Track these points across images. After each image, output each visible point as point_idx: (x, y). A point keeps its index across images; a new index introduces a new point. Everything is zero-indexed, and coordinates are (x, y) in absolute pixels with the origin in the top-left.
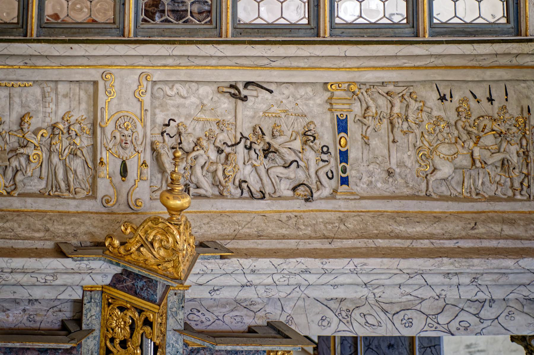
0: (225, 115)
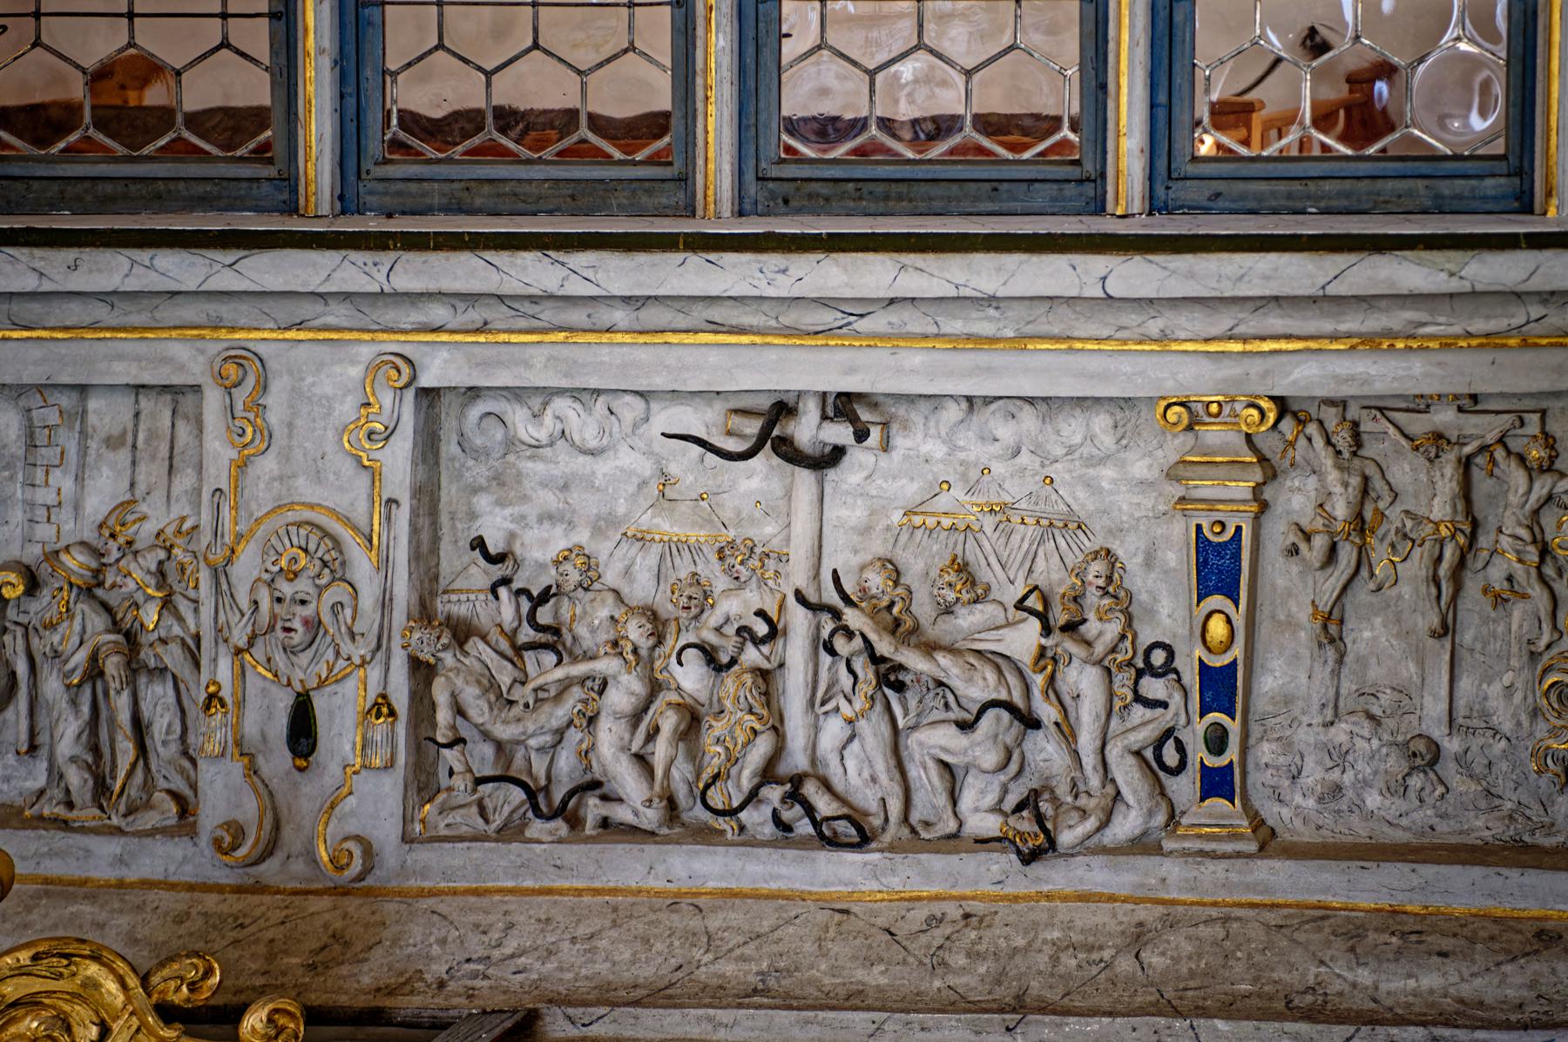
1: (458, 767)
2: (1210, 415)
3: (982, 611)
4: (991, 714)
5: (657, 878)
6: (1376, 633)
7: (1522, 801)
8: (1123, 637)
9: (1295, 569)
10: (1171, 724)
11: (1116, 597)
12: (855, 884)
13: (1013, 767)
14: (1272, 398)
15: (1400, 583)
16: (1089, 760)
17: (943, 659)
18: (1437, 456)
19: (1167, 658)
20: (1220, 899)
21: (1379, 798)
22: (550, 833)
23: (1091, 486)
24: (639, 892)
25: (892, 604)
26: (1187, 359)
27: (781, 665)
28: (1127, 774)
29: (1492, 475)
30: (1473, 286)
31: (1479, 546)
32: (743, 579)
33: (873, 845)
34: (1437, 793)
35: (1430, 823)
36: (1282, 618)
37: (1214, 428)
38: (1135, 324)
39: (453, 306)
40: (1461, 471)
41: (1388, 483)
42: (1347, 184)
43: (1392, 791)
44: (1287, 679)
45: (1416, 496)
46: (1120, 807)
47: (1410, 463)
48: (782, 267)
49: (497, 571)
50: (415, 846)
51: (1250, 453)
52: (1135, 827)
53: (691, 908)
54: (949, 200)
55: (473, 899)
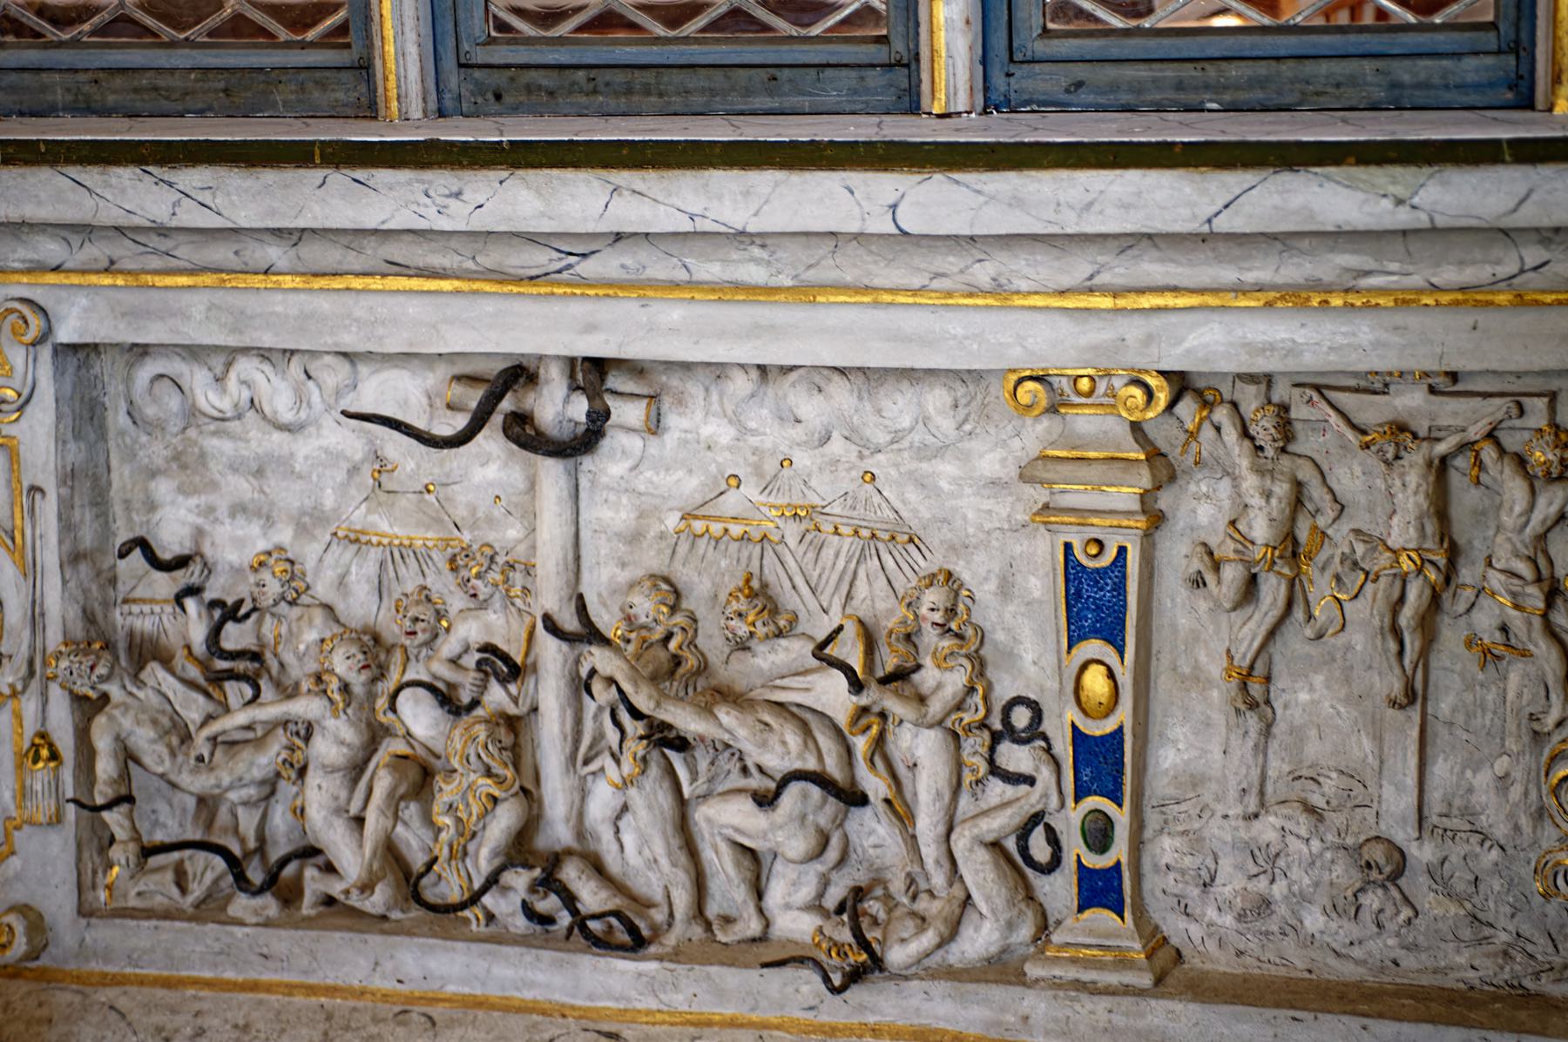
0: (490, 520)
1: (121, 834)
3: (787, 649)
4: (795, 788)
5: (384, 977)
6: (1316, 696)
8: (971, 690)
9: (1203, 606)
10: (1039, 807)
12: (629, 1000)
13: (832, 854)
15: (1348, 628)
16: (930, 851)
17: (726, 715)
18: (1397, 457)
19: (1032, 719)
21: (1322, 919)
22: (256, 913)
23: (922, 483)
24: (362, 993)
25: (668, 637)
26: (1039, 317)
27: (535, 710)
28: (979, 873)
29: (1478, 482)
30: (1432, 220)
31: (1461, 581)
32: (481, 597)
33: (652, 949)
35: (1393, 955)
36: (1187, 670)
38: (956, 270)
39: (65, 239)
40: (1432, 479)
41: (1331, 491)
42: (1262, 69)
43: (1340, 909)
44: (1194, 753)
46: (971, 916)
47: (1361, 464)
48: (455, 189)
49: (182, 578)
50: (93, 921)
52: (990, 944)
53: (423, 1019)
54: (713, 92)
55: (160, 993)
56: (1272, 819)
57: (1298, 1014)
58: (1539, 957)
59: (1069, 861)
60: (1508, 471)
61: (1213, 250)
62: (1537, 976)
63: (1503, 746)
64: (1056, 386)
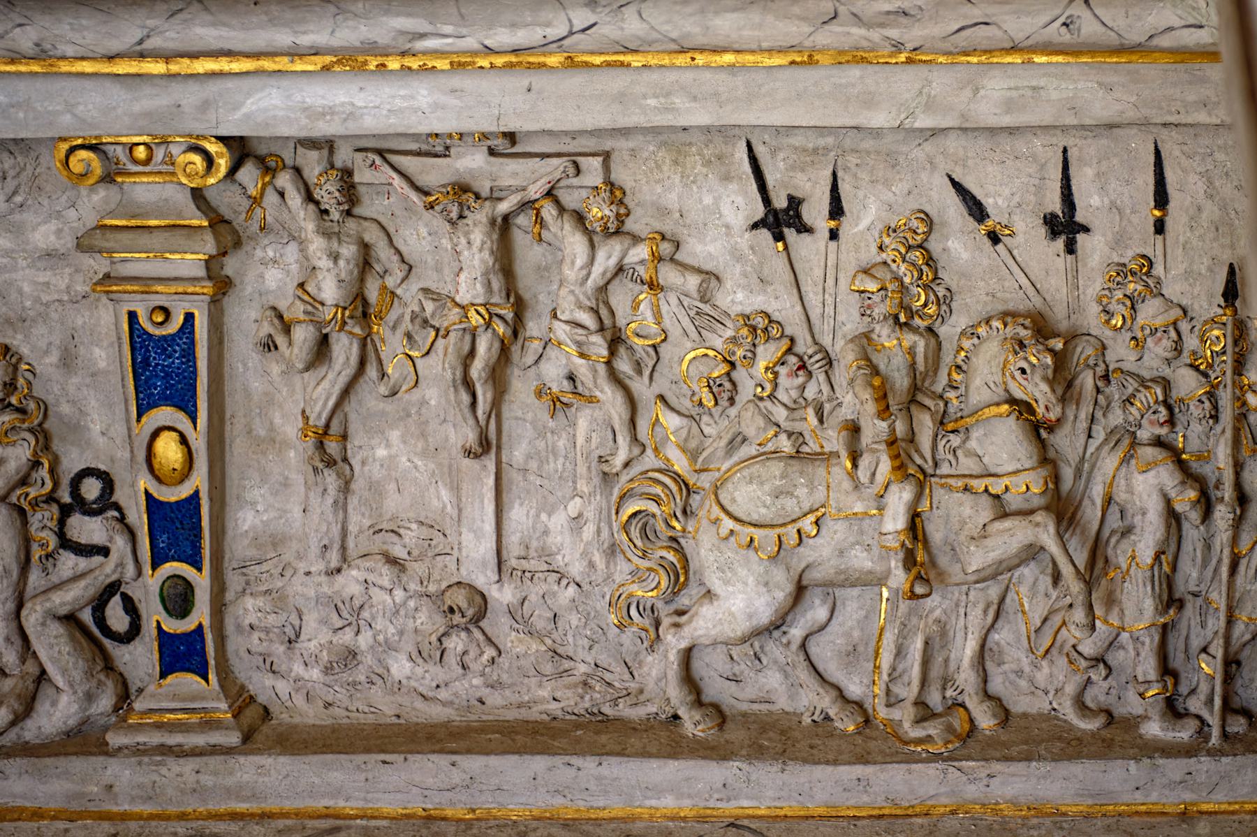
2: (135, 161)
6: (393, 451)
7: (599, 662)
8: (36, 464)
9: (276, 369)
10: (114, 578)
11: (22, 411)
14: (221, 139)
15: (422, 383)
18: (461, 217)
19: (103, 490)
20: (190, 810)
21: (408, 665)
26: (88, 84)
29: (541, 240)
31: (528, 334)
34: (486, 657)
35: (478, 695)
36: (262, 433)
37: (145, 179)
40: (495, 236)
43: (425, 655)
44: (272, 514)
45: (438, 269)
46: (46, 690)
51: (199, 213)
52: (69, 717)
56: (354, 573)
57: (388, 757)
58: (616, 684)
59: (149, 629)
60: (567, 227)
61: (266, 13)
62: (615, 702)
63: (575, 489)
64: (111, 154)
